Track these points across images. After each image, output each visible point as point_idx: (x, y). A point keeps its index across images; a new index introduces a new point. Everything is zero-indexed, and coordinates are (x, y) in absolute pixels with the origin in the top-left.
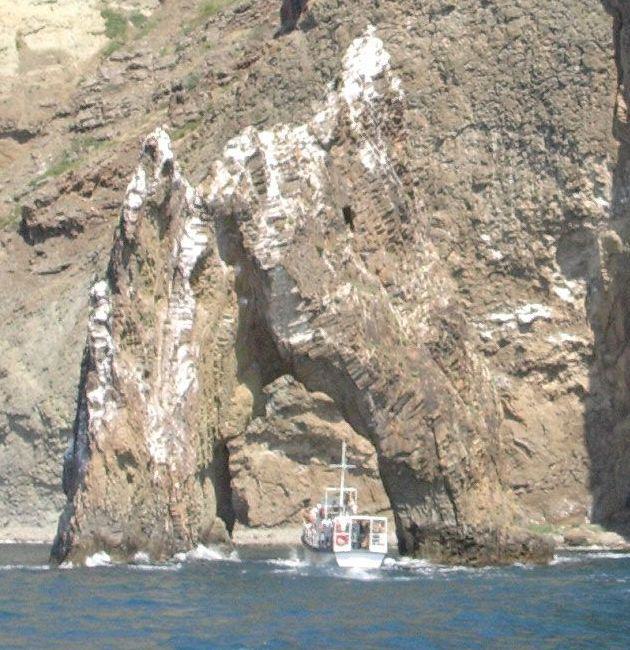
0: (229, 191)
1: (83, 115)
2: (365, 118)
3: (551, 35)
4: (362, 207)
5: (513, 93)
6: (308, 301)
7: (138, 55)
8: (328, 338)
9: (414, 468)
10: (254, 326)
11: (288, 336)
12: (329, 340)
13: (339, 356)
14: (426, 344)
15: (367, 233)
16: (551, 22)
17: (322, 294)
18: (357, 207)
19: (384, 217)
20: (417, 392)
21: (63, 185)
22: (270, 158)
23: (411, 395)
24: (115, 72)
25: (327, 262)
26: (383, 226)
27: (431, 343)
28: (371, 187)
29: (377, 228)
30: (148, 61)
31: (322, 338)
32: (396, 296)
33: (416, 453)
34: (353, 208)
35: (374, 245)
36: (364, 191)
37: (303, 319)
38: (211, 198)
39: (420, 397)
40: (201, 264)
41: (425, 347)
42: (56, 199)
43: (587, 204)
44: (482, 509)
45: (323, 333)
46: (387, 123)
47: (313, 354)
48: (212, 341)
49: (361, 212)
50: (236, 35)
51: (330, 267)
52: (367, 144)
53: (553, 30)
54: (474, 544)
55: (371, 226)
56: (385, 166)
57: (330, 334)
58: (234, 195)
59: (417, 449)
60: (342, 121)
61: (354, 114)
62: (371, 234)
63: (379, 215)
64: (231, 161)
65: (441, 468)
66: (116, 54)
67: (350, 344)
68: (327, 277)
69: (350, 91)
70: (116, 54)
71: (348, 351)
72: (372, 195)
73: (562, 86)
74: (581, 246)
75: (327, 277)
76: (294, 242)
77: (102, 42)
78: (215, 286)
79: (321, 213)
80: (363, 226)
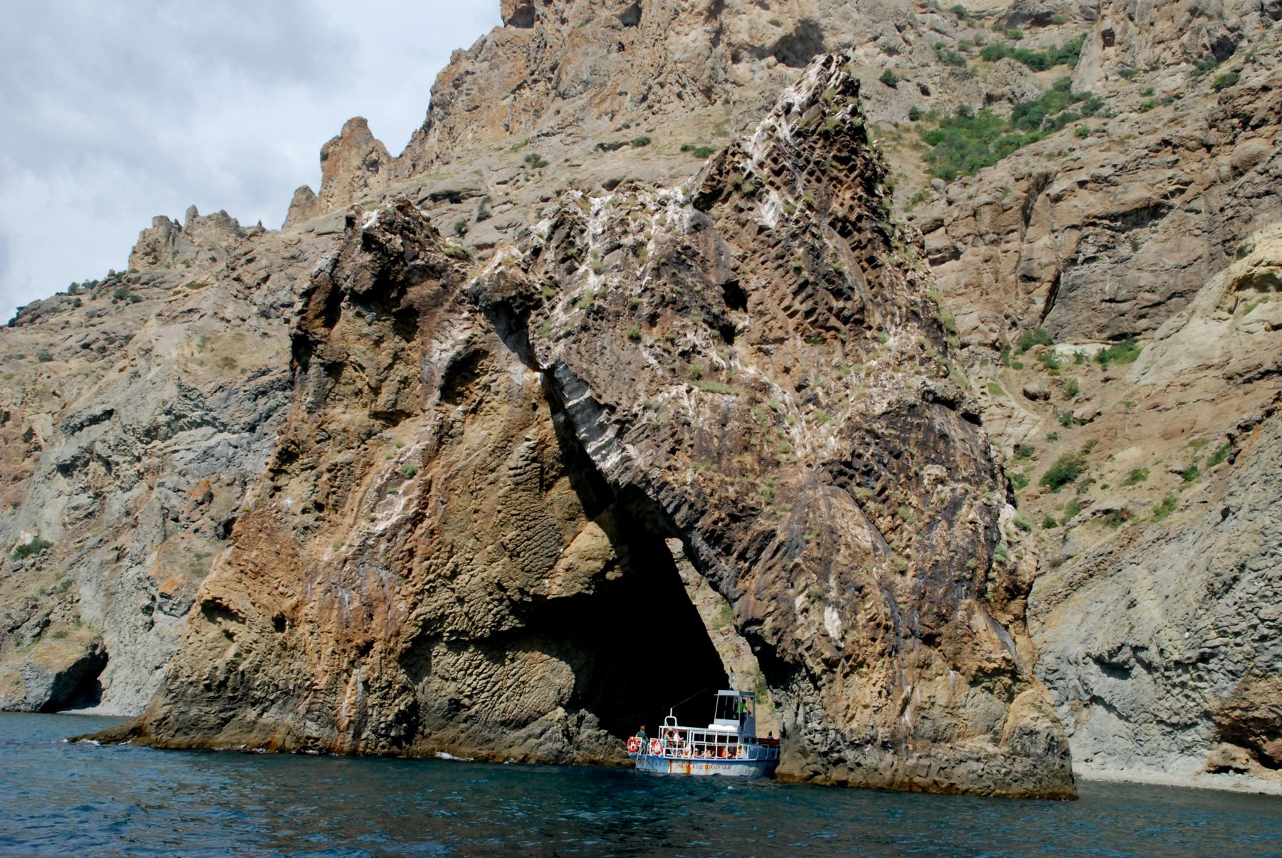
2: (775, 161)
6: (612, 409)
8: (639, 455)
9: (769, 641)
11: (604, 458)
14: (823, 464)
15: (768, 317)
18: (751, 282)
19: (795, 294)
20: (778, 532)
21: (1268, 408)
23: (771, 535)
25: (645, 354)
26: (797, 306)
27: (832, 462)
28: (773, 252)
29: (786, 309)
31: (629, 459)
32: (809, 401)
33: (769, 620)
34: (742, 284)
35: (780, 334)
36: (762, 259)
37: (610, 433)
39: (781, 537)
41: (822, 468)
42: (1260, 422)
44: (866, 707)
45: (632, 450)
46: (817, 163)
47: (624, 480)
48: (492, 471)
49: (757, 289)
51: (653, 361)
52: (774, 196)
54: (842, 760)
55: (772, 305)
56: (797, 222)
59: (770, 614)
62: (774, 318)
63: (788, 291)
65: (797, 643)
67: (667, 464)
68: (647, 374)
72: (775, 265)
75: (647, 374)
76: (585, 328)
78: (497, 398)
80: (760, 307)
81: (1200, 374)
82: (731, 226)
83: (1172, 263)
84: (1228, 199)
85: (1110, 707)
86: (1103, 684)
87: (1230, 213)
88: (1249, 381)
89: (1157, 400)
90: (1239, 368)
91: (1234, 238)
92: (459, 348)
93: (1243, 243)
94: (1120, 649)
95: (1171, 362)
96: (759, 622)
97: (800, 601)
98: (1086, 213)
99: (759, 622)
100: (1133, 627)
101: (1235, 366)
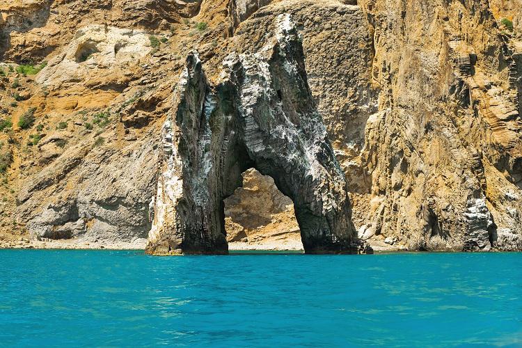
0: (227, 80)
1: (143, 78)
3: (344, 36)
4: (285, 90)
5: (328, 61)
7: (165, 54)
10: (237, 144)
12: (273, 151)
13: (278, 158)
16: (344, 30)
17: (269, 129)
22: (245, 65)
24: (155, 61)
30: (168, 57)
31: (270, 150)
38: (218, 82)
40: (214, 113)
43: (360, 108)
47: (266, 156)
50: (205, 45)
53: (345, 34)
57: (273, 148)
58: (229, 81)
60: (276, 48)
61: (282, 46)
64: (226, 66)
66: (156, 54)
69: (278, 37)
70: (156, 54)
71: (282, 155)
73: (349, 57)
74: (357, 125)
77: (150, 49)
79: (268, 92)
81: (72, 83)
82: (279, 72)
83: (47, 33)
84: (70, 10)
85: (107, 221)
86: (102, 211)
87: (72, 17)
88: (96, 89)
89: (57, 92)
90: (91, 82)
91: (74, 27)
92: (212, 108)
93: (79, 29)
94: (111, 198)
95: (59, 77)
96: (309, 203)
97: (325, 198)
98: (11, 6)
99: (309, 203)
100: (117, 190)
101: (88, 81)
